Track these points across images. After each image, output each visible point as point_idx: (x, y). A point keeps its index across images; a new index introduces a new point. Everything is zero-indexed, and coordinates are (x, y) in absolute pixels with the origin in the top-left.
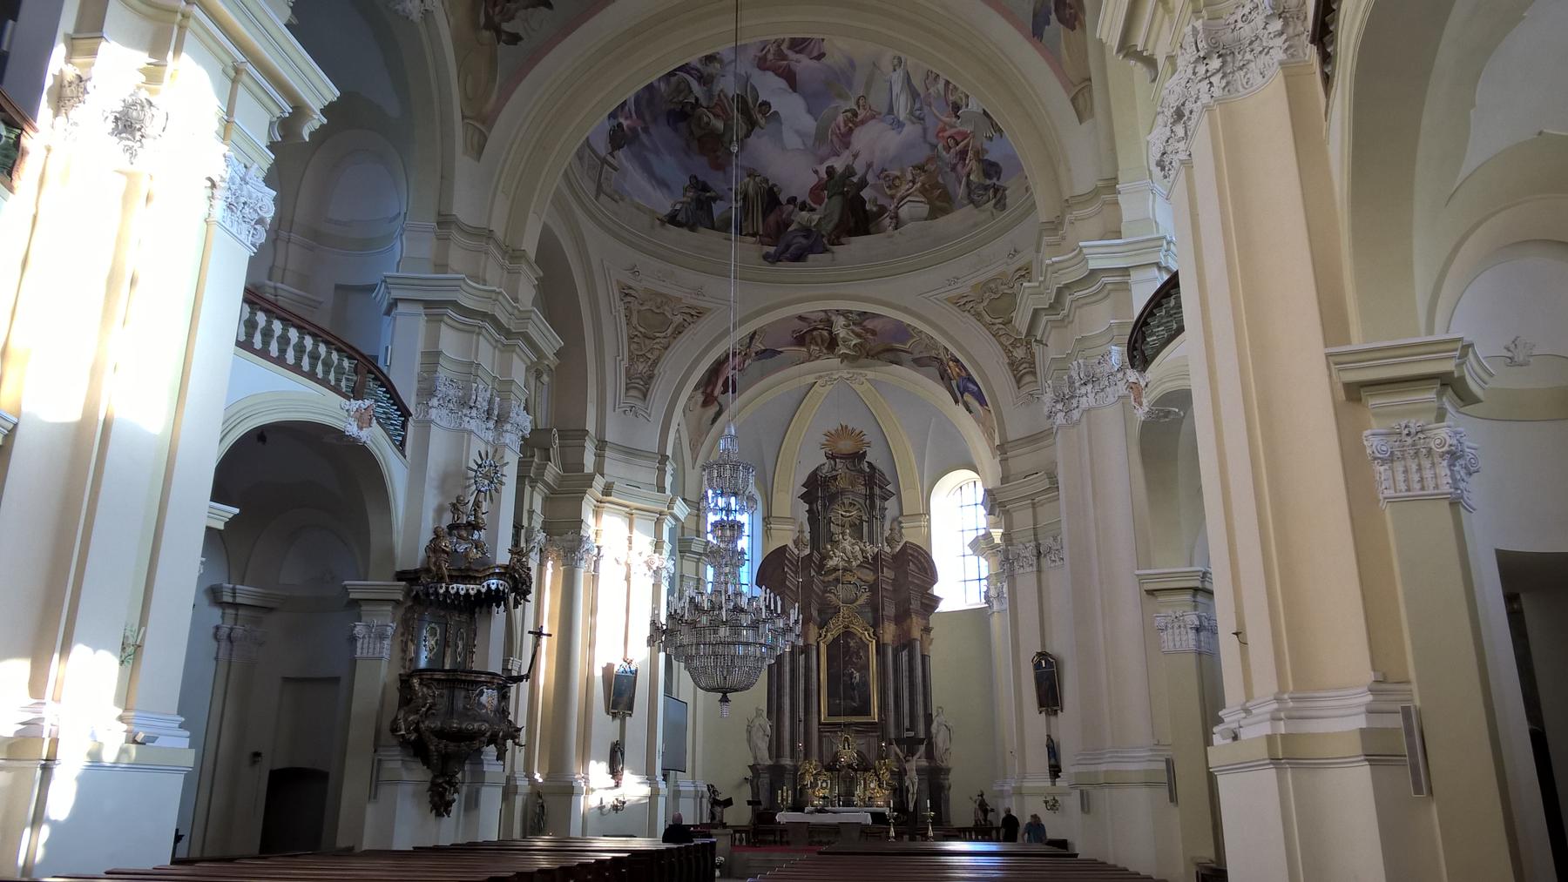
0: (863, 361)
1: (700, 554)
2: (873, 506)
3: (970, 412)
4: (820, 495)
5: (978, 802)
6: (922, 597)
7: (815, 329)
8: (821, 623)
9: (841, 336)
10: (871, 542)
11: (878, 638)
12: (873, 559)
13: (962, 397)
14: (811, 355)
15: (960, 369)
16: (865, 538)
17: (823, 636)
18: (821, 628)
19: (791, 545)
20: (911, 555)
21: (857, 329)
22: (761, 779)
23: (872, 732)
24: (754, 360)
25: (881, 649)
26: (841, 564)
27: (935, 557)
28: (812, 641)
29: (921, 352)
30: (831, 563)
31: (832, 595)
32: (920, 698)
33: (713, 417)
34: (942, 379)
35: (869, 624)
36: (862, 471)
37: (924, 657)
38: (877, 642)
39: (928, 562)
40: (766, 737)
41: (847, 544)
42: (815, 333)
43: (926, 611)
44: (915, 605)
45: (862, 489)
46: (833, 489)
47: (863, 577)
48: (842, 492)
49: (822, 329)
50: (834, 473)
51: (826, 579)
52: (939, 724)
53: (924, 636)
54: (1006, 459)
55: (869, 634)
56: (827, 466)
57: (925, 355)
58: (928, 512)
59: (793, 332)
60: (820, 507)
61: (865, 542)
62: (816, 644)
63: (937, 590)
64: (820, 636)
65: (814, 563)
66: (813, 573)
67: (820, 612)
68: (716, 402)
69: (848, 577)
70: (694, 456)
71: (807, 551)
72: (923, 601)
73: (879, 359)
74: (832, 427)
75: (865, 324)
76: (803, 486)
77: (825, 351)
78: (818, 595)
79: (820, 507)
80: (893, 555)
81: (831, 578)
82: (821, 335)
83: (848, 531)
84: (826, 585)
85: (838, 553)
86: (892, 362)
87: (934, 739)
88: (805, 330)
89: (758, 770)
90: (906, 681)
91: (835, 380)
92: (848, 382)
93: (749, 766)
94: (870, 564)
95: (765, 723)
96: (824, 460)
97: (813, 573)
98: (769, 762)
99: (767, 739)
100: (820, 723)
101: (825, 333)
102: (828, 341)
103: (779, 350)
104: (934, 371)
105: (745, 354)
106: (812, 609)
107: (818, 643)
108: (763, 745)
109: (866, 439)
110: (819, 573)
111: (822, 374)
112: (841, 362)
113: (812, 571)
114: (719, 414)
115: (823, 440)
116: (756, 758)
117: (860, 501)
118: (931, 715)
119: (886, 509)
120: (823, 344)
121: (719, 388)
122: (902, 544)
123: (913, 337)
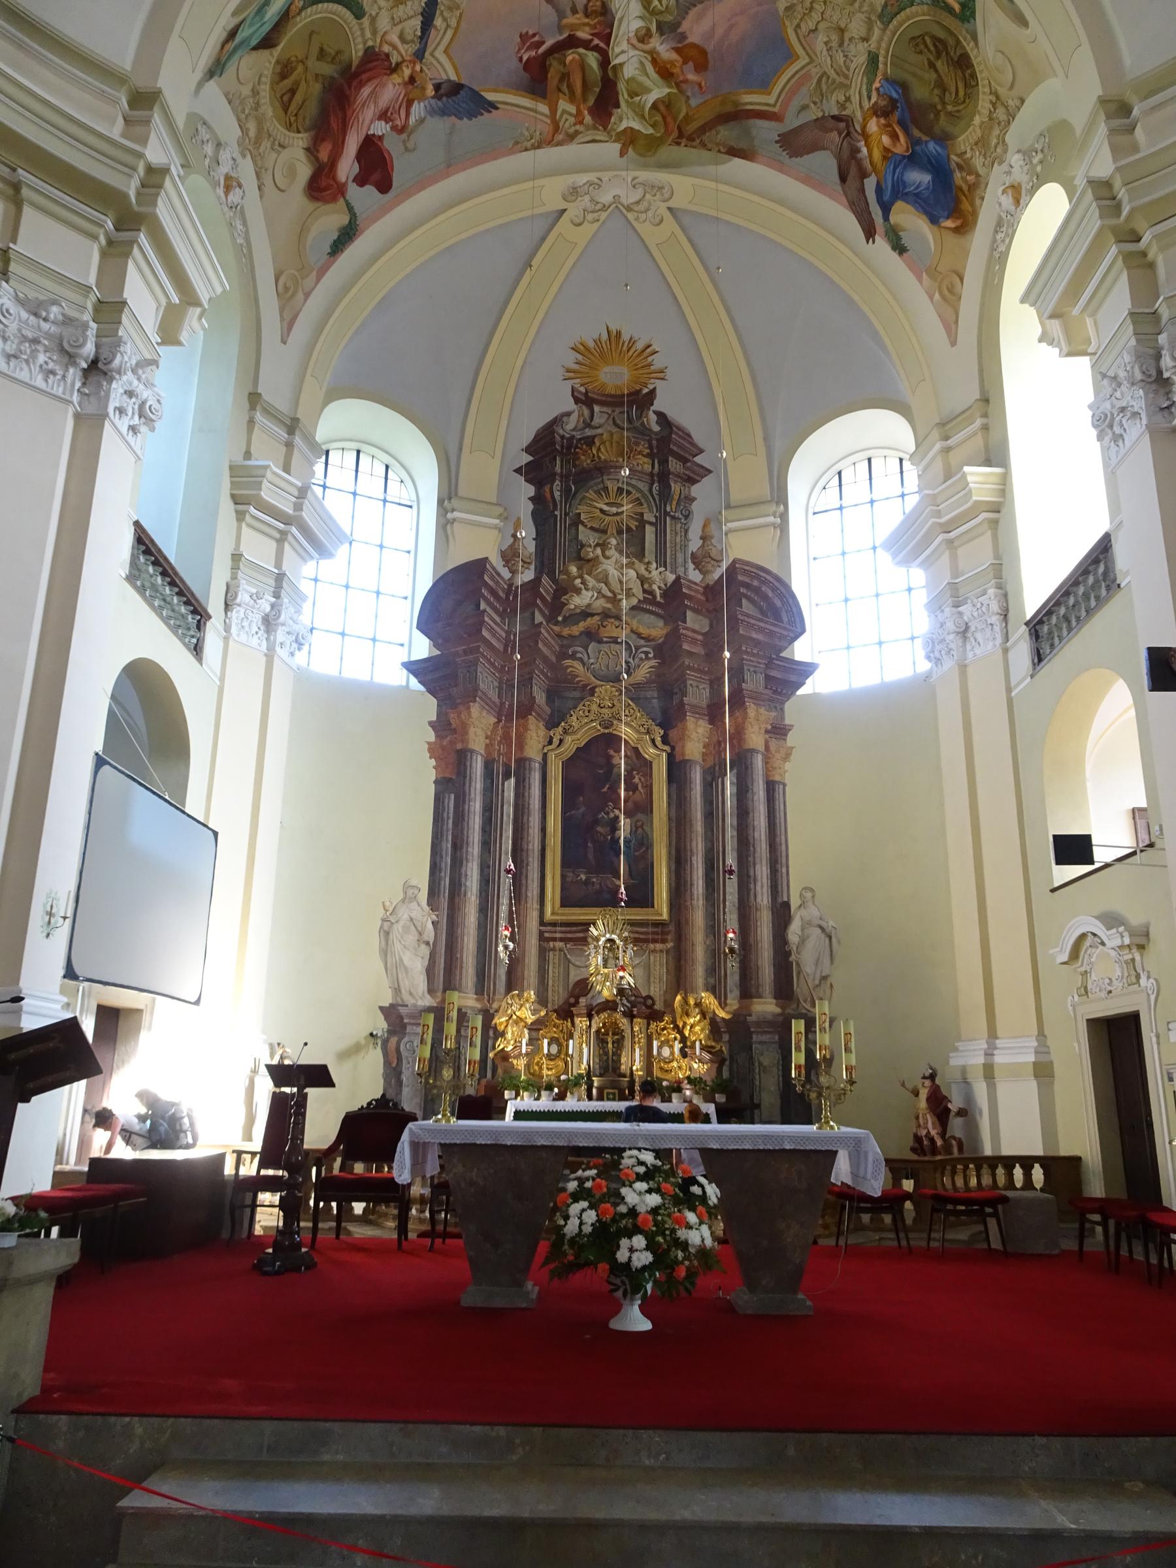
0: (669, 152)
1: (287, 520)
2: (665, 495)
3: (900, 248)
4: (558, 469)
5: (924, 1094)
6: (770, 664)
7: (572, 42)
8: (551, 716)
9: (629, 71)
10: (662, 562)
11: (673, 748)
12: (665, 594)
13: (886, 218)
14: (556, 129)
15: (894, 137)
16: (650, 555)
17: (556, 741)
18: (551, 724)
19: (496, 561)
20: (747, 586)
21: (664, 49)
22: (406, 1039)
23: (655, 941)
24: (432, 112)
25: (677, 770)
26: (600, 604)
27: (798, 586)
28: (533, 748)
29: (804, 108)
30: (578, 601)
31: (577, 664)
32: (762, 871)
33: (335, 237)
34: (843, 179)
35: (654, 720)
36: (644, 431)
37: (771, 787)
38: (671, 757)
39: (781, 596)
40: (423, 946)
41: (609, 567)
42: (571, 56)
43: (775, 692)
44: (754, 682)
45: (645, 464)
46: (585, 462)
47: (641, 630)
48: (603, 469)
49: (586, 45)
50: (589, 432)
51: (566, 632)
52: (806, 925)
53: (773, 745)
54: (1131, 129)
55: (653, 741)
56: (574, 417)
57: (814, 113)
58: (780, 496)
59: (524, 37)
60: (557, 494)
61: (649, 563)
62: (539, 758)
63: (801, 651)
64: (550, 743)
65: (543, 599)
66: (539, 618)
67: (551, 695)
68: (342, 200)
69: (610, 630)
70: (288, 316)
71: (528, 575)
72: (773, 673)
73: (703, 145)
74: (591, 332)
75: (685, 26)
76: (528, 450)
77: (588, 119)
78: (545, 659)
79: (557, 494)
80: (707, 587)
81: (576, 630)
82: (583, 66)
83: (614, 542)
84: (565, 642)
85: (591, 582)
86: (734, 152)
87: (793, 958)
88: (549, 43)
89: (401, 1018)
90: (730, 834)
91: (604, 208)
92: (630, 216)
93: (381, 1008)
94: (658, 604)
95: (422, 915)
96: (570, 405)
97: (539, 618)
98: (428, 1001)
99: (425, 951)
100: (542, 923)
101: (592, 59)
102: (597, 90)
103: (490, 96)
104: (825, 162)
105: (412, 80)
106: (535, 688)
107: (545, 755)
108: (415, 963)
109: (658, 362)
110: (551, 619)
111: (582, 179)
112: (622, 154)
113: (537, 614)
114: (346, 236)
115: (570, 359)
116: (397, 990)
117: (641, 485)
118: (787, 905)
119: (694, 499)
120: (585, 100)
121: (347, 167)
122: (724, 566)
123: (791, 56)
